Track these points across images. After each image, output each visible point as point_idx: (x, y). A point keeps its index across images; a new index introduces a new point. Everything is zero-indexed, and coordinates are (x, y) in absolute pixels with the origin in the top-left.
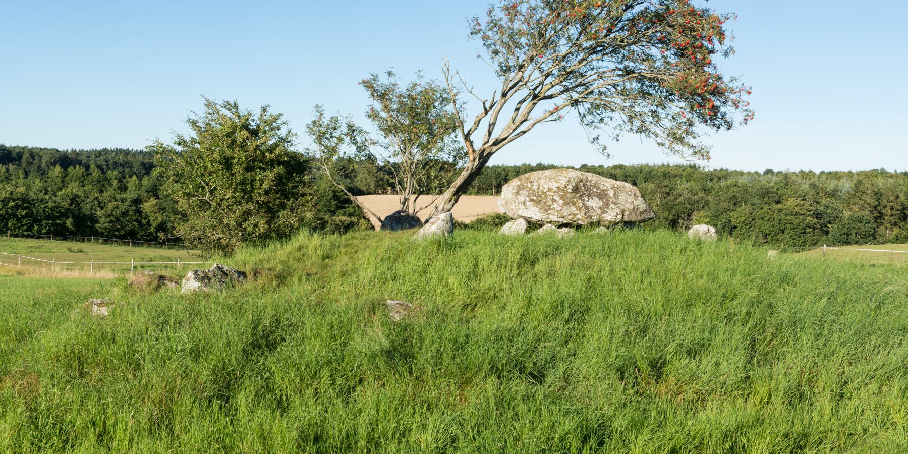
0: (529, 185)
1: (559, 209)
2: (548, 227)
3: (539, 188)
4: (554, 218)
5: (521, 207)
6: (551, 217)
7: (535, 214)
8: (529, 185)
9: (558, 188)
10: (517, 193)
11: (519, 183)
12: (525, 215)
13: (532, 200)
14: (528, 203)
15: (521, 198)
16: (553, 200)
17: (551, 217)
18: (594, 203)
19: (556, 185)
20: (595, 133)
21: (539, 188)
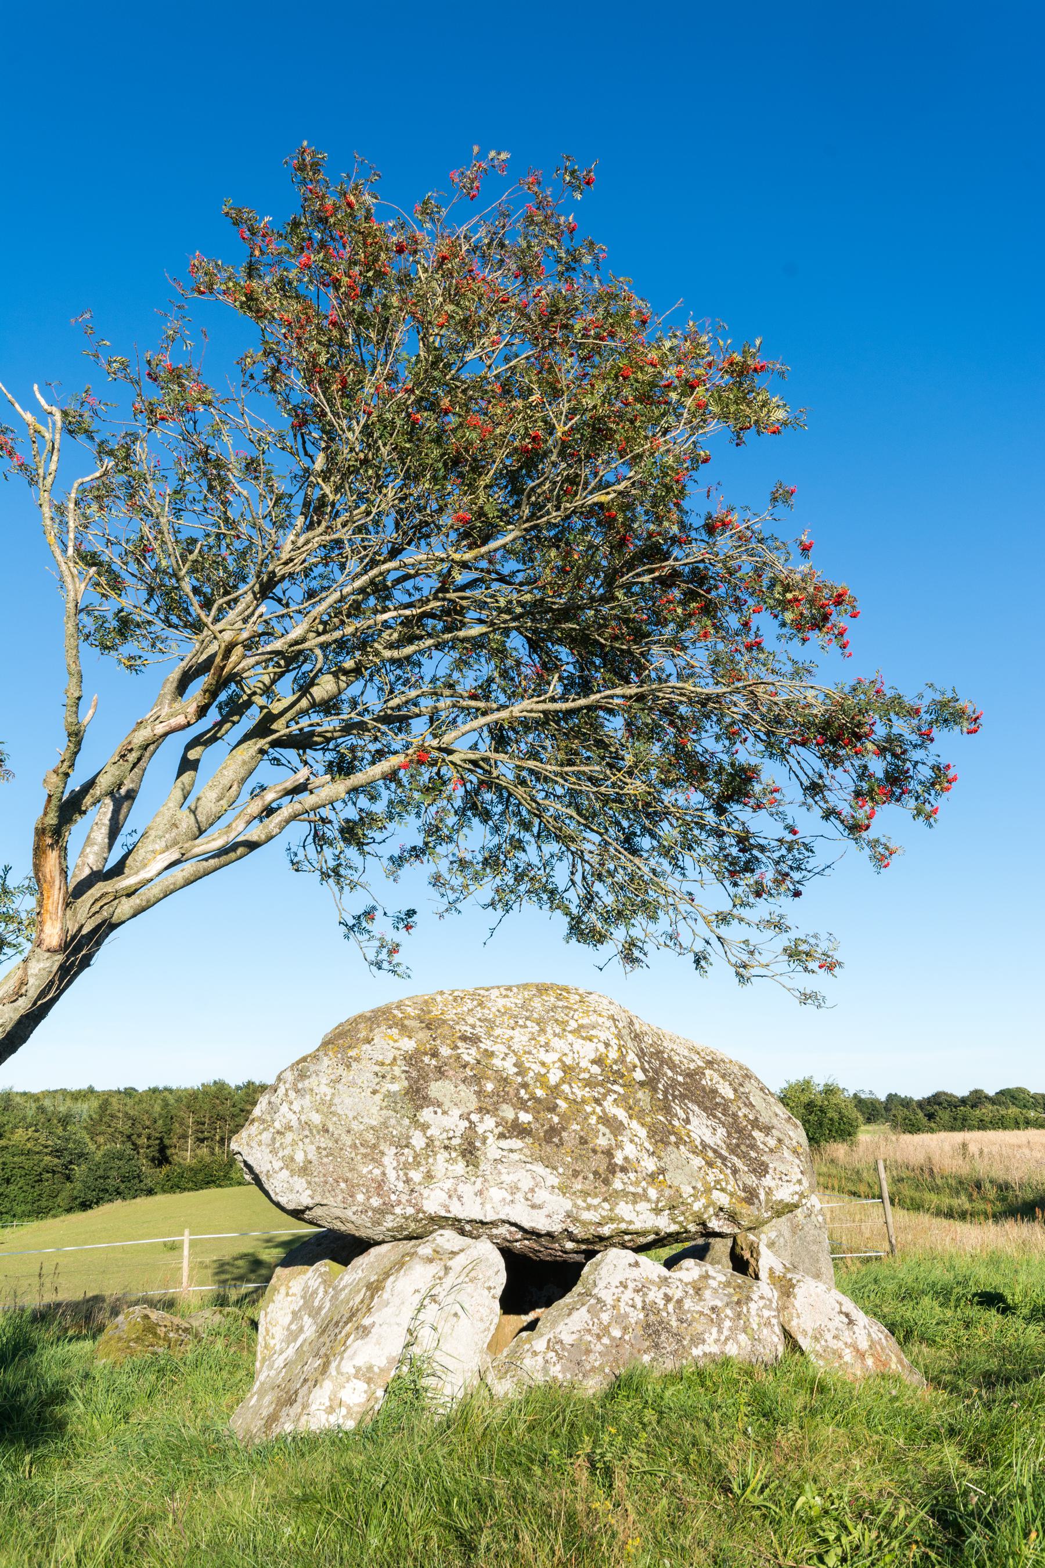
0: (469, 1054)
1: (650, 1165)
2: (612, 1273)
3: (521, 1069)
4: (642, 1218)
5: (447, 1167)
6: (624, 1209)
7: (538, 1200)
8: (469, 1054)
9: (598, 1061)
10: (417, 1096)
11: (408, 1045)
12: (469, 1210)
13: (518, 1130)
14: (492, 1149)
15: (445, 1123)
16: (616, 1127)
17: (624, 1209)
18: (702, 1128)
19: (587, 1051)
20: (355, 903)
21: (522, 1070)
